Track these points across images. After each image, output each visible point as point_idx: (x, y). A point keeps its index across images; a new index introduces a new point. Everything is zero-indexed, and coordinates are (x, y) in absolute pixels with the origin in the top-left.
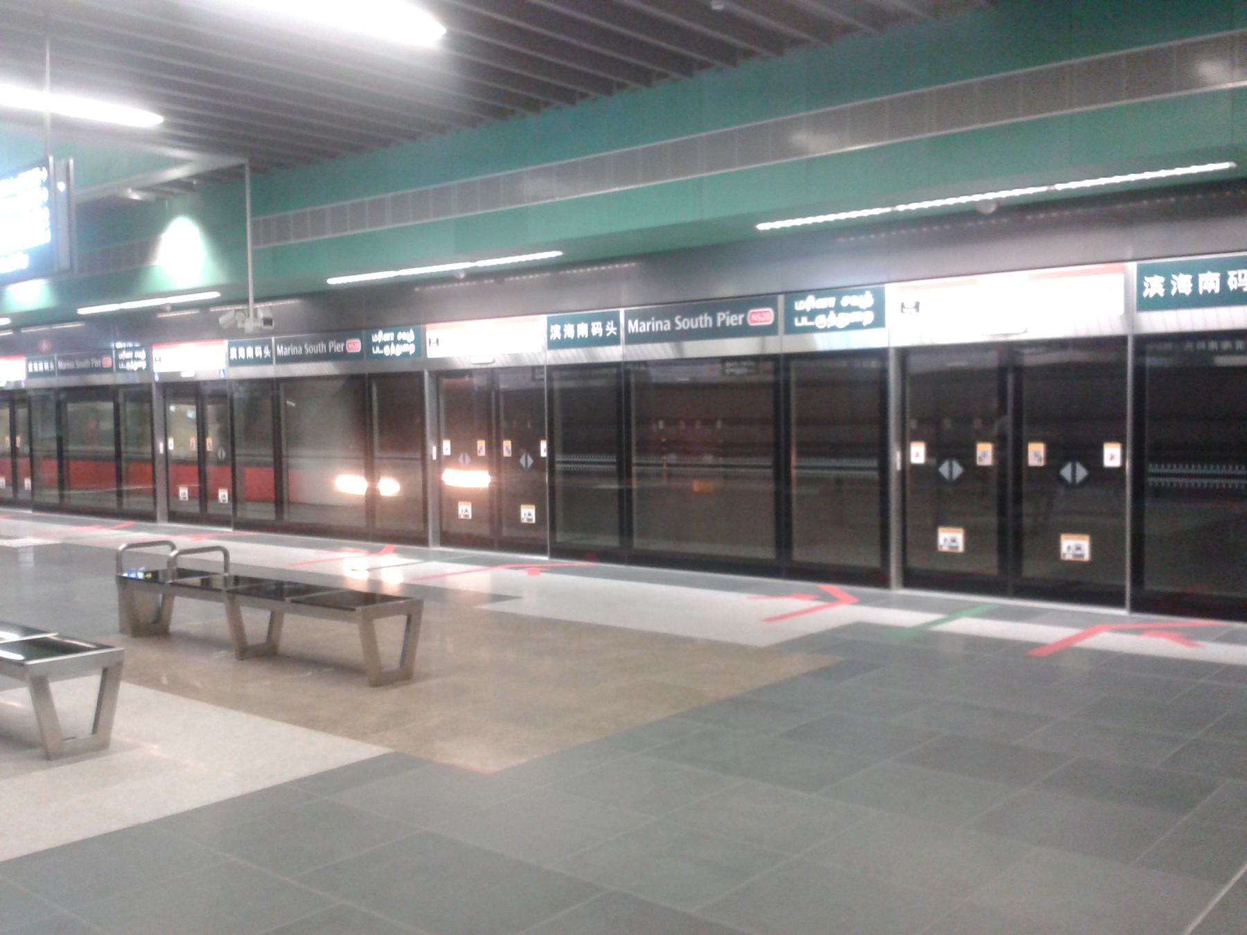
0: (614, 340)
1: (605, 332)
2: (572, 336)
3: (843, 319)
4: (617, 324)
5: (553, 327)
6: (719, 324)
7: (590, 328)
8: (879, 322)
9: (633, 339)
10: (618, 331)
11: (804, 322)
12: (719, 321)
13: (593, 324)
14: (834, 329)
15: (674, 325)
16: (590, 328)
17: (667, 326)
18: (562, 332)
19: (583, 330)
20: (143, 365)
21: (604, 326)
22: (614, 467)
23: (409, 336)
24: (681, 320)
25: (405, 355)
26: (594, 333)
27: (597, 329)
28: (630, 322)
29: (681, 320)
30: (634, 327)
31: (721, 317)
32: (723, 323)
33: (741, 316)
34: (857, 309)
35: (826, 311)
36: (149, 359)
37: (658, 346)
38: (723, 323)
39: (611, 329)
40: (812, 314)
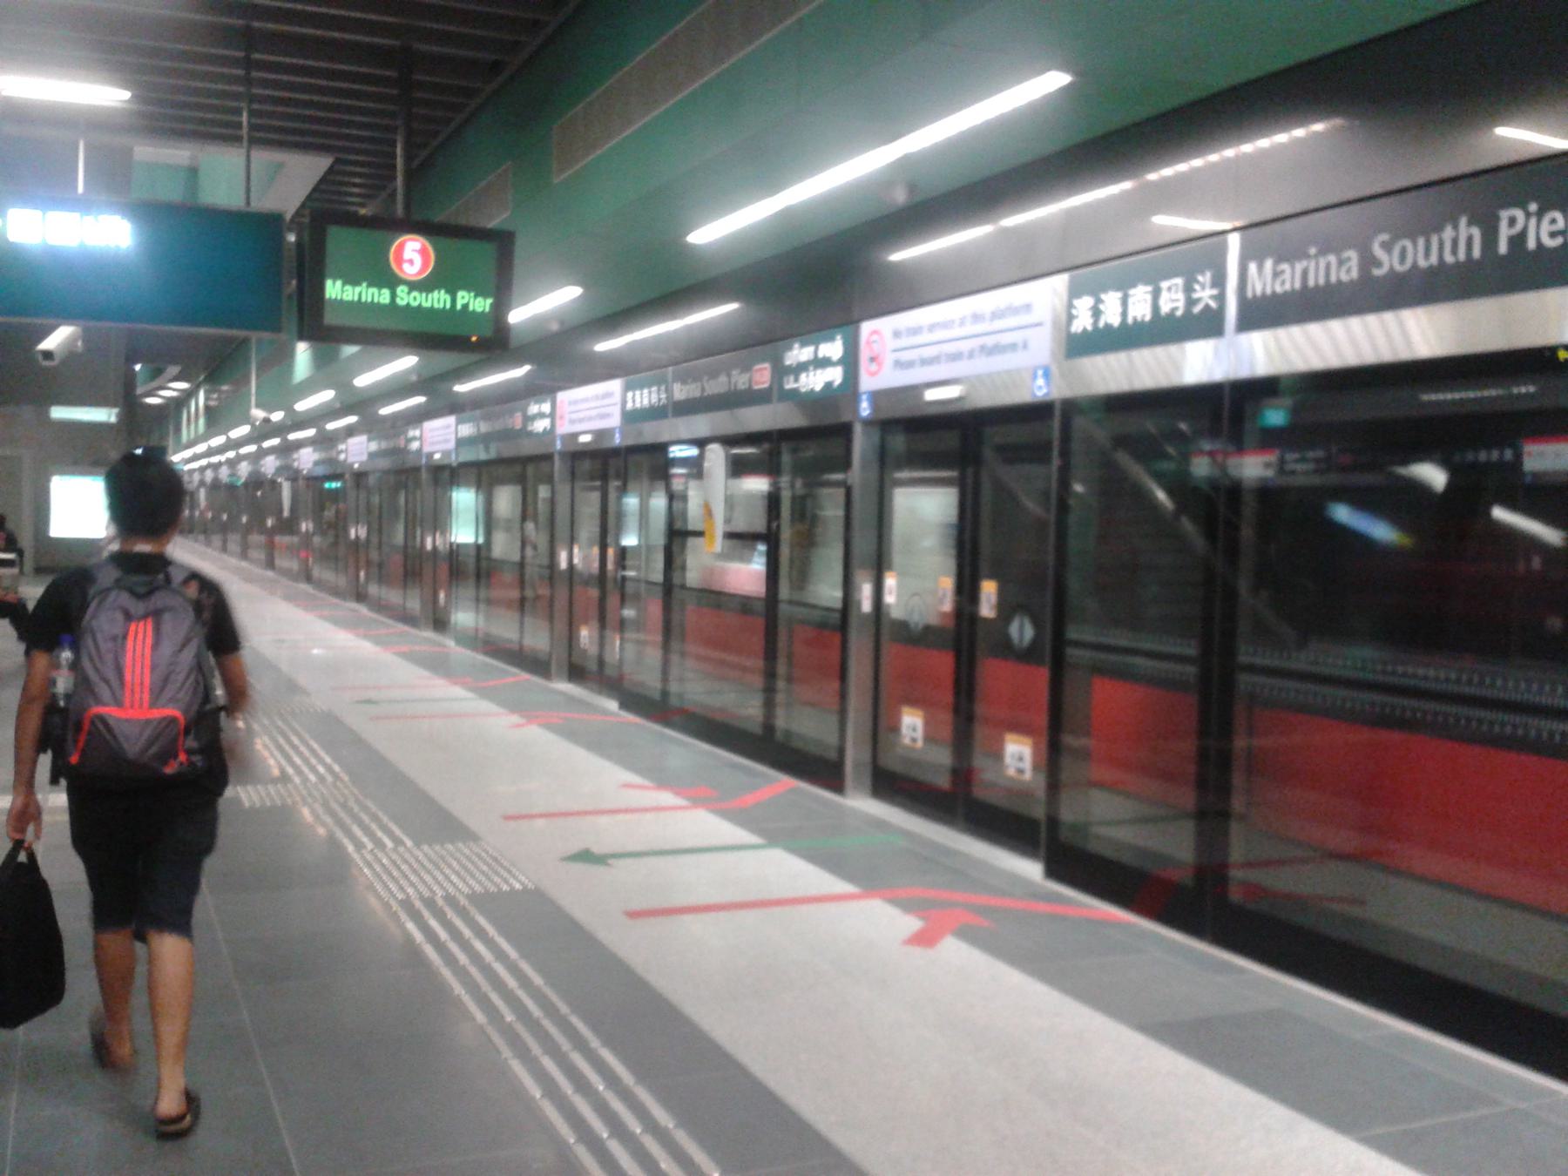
0: (1206, 324)
1: (1191, 302)
2: (1115, 321)
4: (1219, 281)
5: (1076, 302)
6: (1503, 248)
9: (1262, 313)
10: (1221, 298)
12: (1504, 233)
13: (1164, 285)
15: (1368, 261)
17: (1347, 269)
18: (1096, 313)
19: (1140, 306)
20: (835, 375)
22: (1191, 670)
23: (833, 349)
24: (1387, 247)
25: (828, 385)
26: (1165, 308)
27: (1172, 299)
30: (1265, 279)
31: (1512, 221)
32: (1518, 241)
36: (850, 362)
37: (1338, 328)
38: (1518, 241)
39: (1205, 295)
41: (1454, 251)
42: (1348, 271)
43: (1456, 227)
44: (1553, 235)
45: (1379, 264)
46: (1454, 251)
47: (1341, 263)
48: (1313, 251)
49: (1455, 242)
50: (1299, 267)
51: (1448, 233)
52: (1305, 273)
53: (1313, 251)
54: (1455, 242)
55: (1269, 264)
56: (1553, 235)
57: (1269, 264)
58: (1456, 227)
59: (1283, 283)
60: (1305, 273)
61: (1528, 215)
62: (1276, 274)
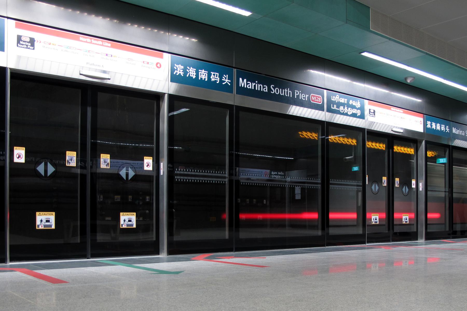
1: (221, 81)
3: (350, 111)
7: (209, 75)
8: (362, 117)
11: (335, 108)
12: (296, 94)
14: (346, 114)
15: (270, 90)
16: (209, 75)
21: (221, 77)
24: (274, 88)
28: (241, 79)
29: (274, 88)
33: (307, 96)
34: (353, 107)
35: (343, 105)
38: (298, 96)
40: (339, 104)
41: (287, 94)
42: (265, 90)
43: (287, 90)
44: (304, 98)
45: (273, 91)
46: (287, 94)
47: (263, 87)
48: (257, 82)
49: (287, 92)
50: (253, 84)
51: (286, 90)
52: (255, 86)
53: (257, 82)
54: (287, 92)
55: (245, 80)
56: (304, 98)
57: (245, 80)
58: (287, 90)
59: (249, 86)
60: (255, 86)
61: (300, 93)
62: (247, 84)
